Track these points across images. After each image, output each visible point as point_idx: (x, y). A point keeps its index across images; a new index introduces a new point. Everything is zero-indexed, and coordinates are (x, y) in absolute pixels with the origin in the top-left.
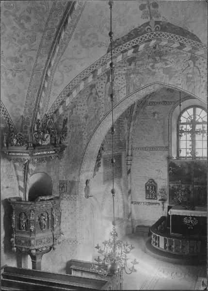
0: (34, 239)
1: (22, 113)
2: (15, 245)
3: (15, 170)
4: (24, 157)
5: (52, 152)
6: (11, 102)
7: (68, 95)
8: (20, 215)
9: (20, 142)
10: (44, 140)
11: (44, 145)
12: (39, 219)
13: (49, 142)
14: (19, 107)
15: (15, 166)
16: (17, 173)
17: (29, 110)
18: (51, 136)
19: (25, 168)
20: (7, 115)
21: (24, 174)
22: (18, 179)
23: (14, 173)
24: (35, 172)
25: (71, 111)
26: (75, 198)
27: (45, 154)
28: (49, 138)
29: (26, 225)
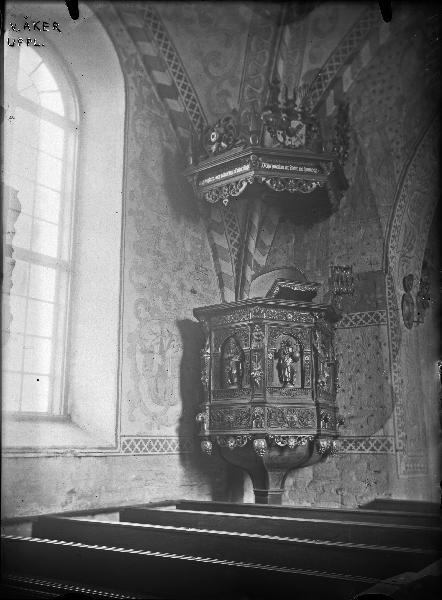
0: (262, 404)
1: (233, 104)
2: (207, 433)
3: (216, 258)
4: (237, 179)
5: (309, 170)
6: (209, 75)
7: (349, 61)
8: (225, 347)
9: (227, 142)
10: (291, 133)
11: (289, 147)
12: (277, 355)
13: (303, 141)
14: (226, 85)
15: (214, 248)
16: (218, 266)
17: (251, 91)
18: (309, 128)
19: (239, 255)
20: (198, 110)
21: (237, 270)
22: (221, 285)
23: (211, 265)
24: (265, 270)
25: (355, 102)
26: (377, 318)
27: (293, 172)
28: (303, 131)
29: (238, 373)
